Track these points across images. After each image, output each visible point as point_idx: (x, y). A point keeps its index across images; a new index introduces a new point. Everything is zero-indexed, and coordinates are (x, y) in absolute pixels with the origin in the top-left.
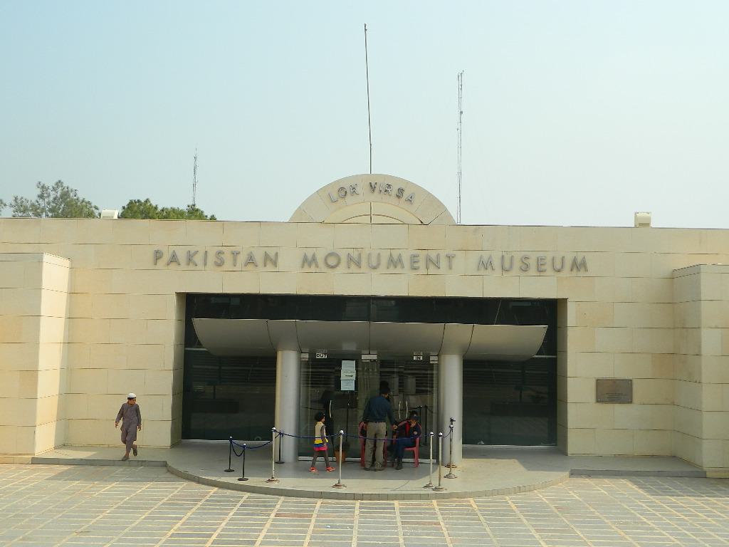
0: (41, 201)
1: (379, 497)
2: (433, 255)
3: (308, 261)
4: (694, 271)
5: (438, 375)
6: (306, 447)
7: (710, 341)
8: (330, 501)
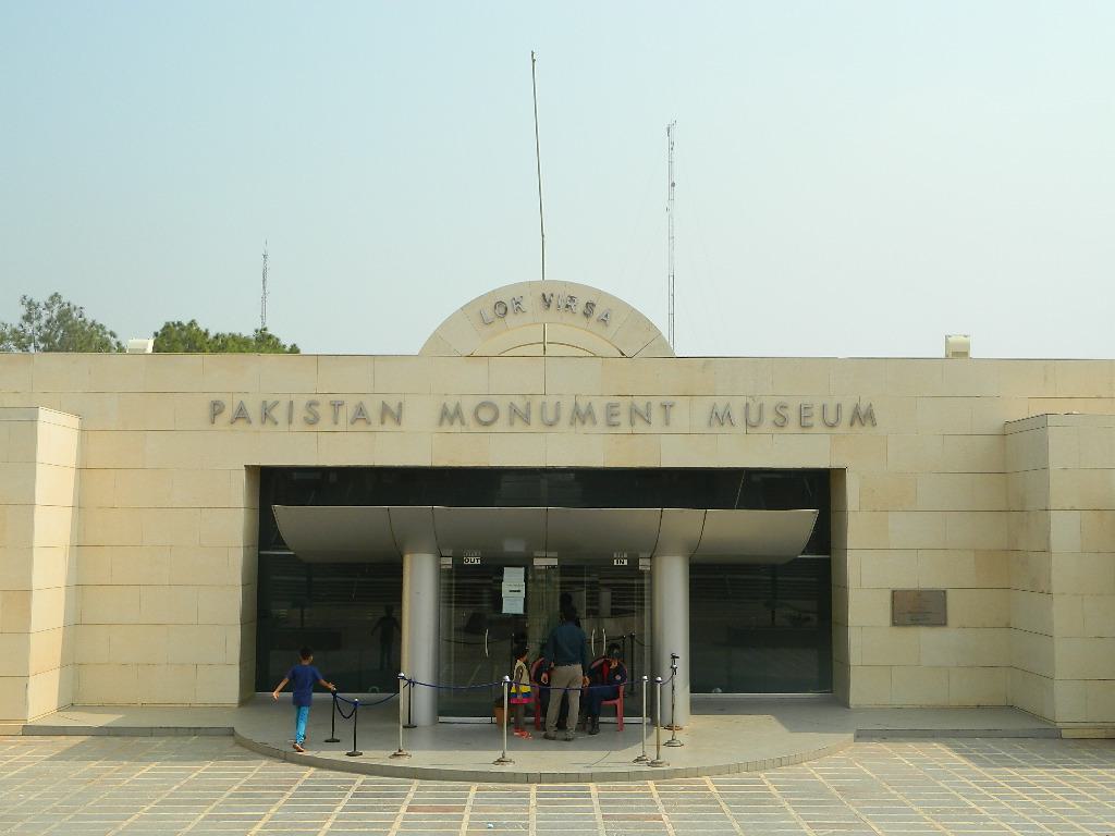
0: (27, 325)
1: (566, 778)
2: (641, 403)
3: (449, 416)
4: (1039, 424)
5: (651, 584)
6: (447, 705)
7: (1065, 532)
8: (490, 785)
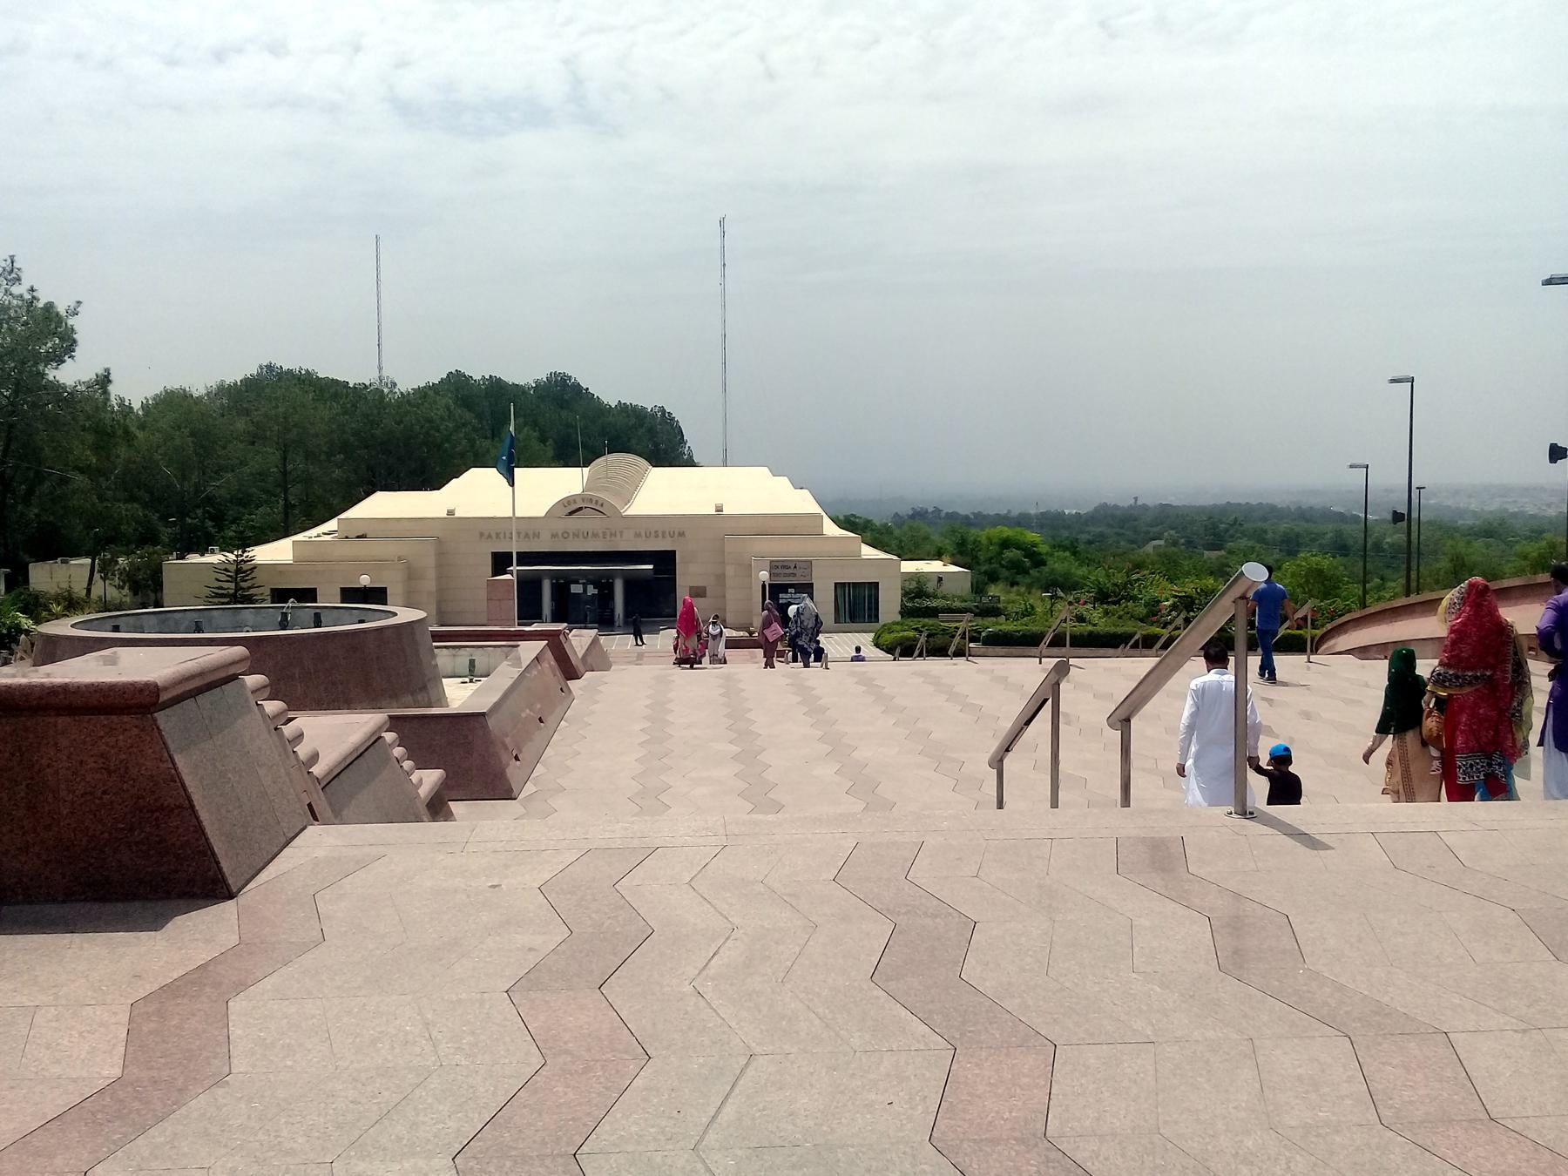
3: (554, 536)
7: (730, 571)
